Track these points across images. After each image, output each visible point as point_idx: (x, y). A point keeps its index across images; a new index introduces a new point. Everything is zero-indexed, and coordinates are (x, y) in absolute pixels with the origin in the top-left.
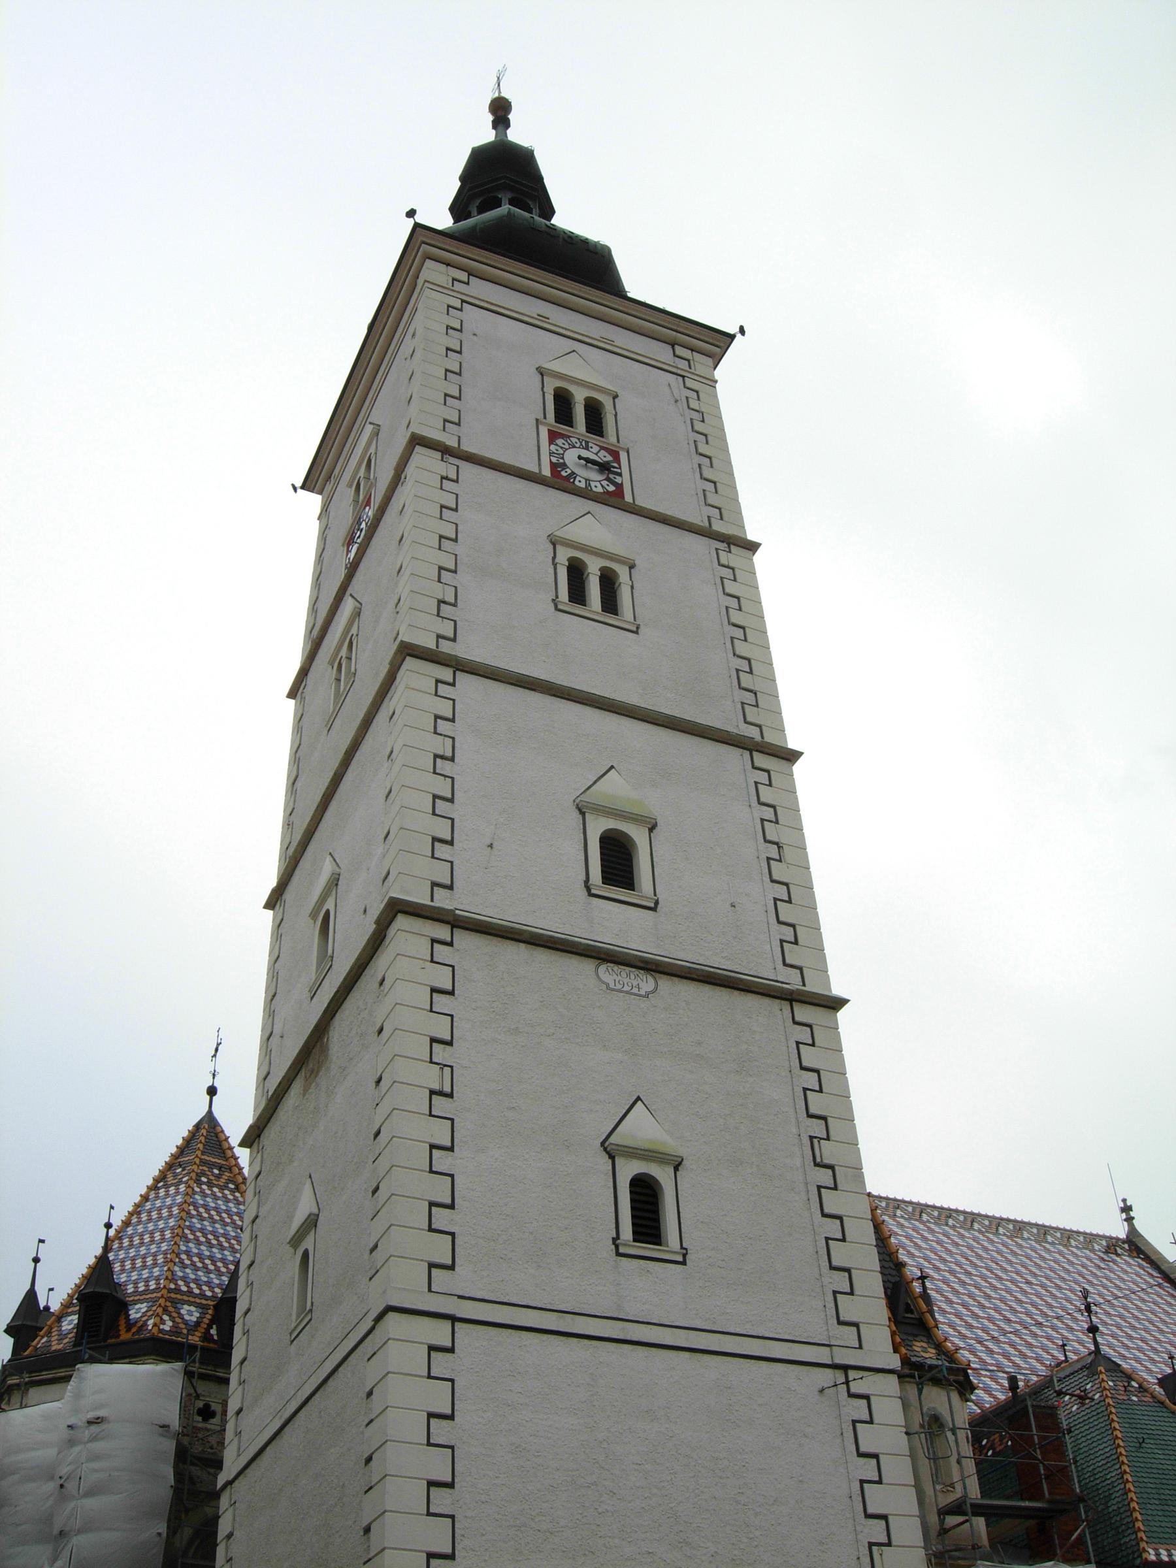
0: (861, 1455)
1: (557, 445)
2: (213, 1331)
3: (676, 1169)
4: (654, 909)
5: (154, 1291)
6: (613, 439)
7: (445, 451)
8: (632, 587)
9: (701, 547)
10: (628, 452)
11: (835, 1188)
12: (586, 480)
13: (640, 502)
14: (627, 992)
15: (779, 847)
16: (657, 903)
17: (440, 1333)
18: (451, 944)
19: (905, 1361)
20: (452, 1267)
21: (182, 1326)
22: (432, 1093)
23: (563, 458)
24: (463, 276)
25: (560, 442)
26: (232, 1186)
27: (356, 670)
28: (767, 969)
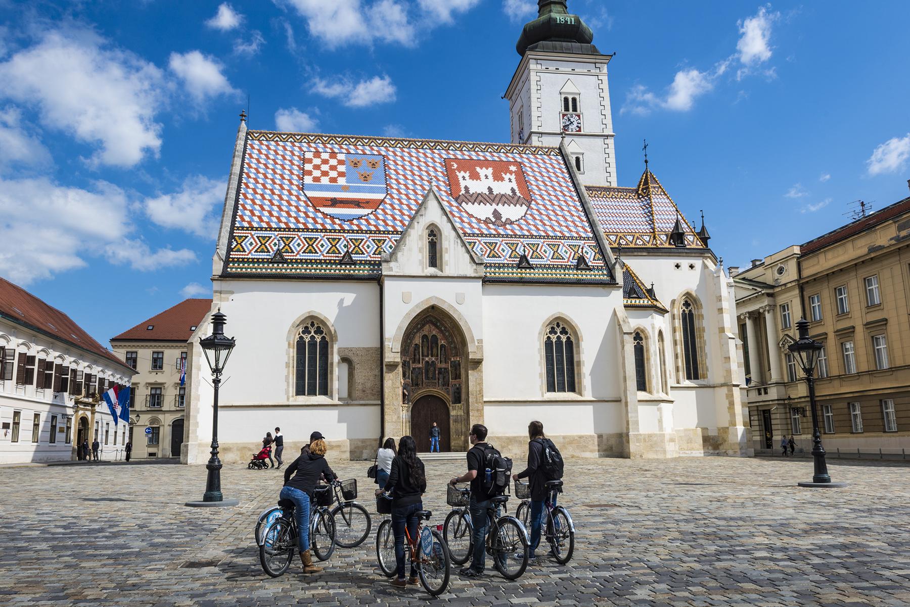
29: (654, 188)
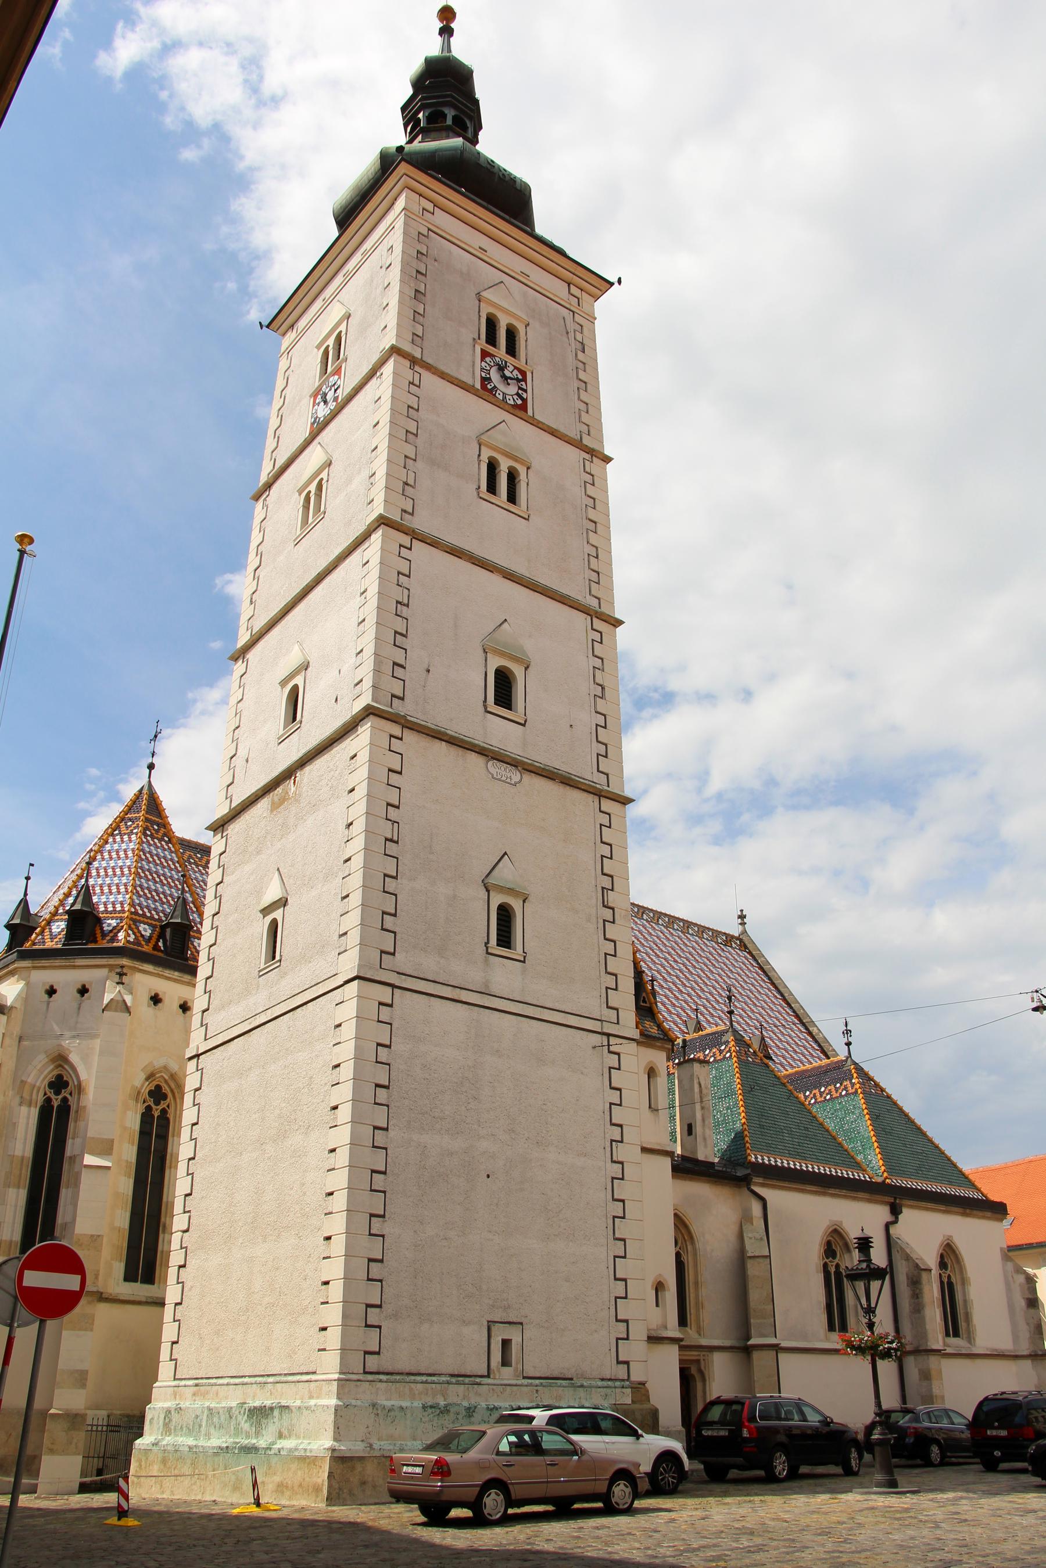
0: (612, 1088)
1: (486, 362)
2: (161, 944)
3: (524, 901)
4: (524, 725)
5: (119, 912)
6: (523, 360)
8: (528, 484)
9: (574, 455)
10: (532, 373)
11: (613, 922)
12: (503, 393)
14: (503, 781)
15: (602, 688)
16: (526, 721)
18: (401, 739)
19: (642, 1034)
20: (393, 954)
21: (141, 939)
22: (387, 839)
23: (489, 374)
24: (430, 206)
25: (488, 359)
26: (166, 839)
28: (583, 769)
29: (153, 823)
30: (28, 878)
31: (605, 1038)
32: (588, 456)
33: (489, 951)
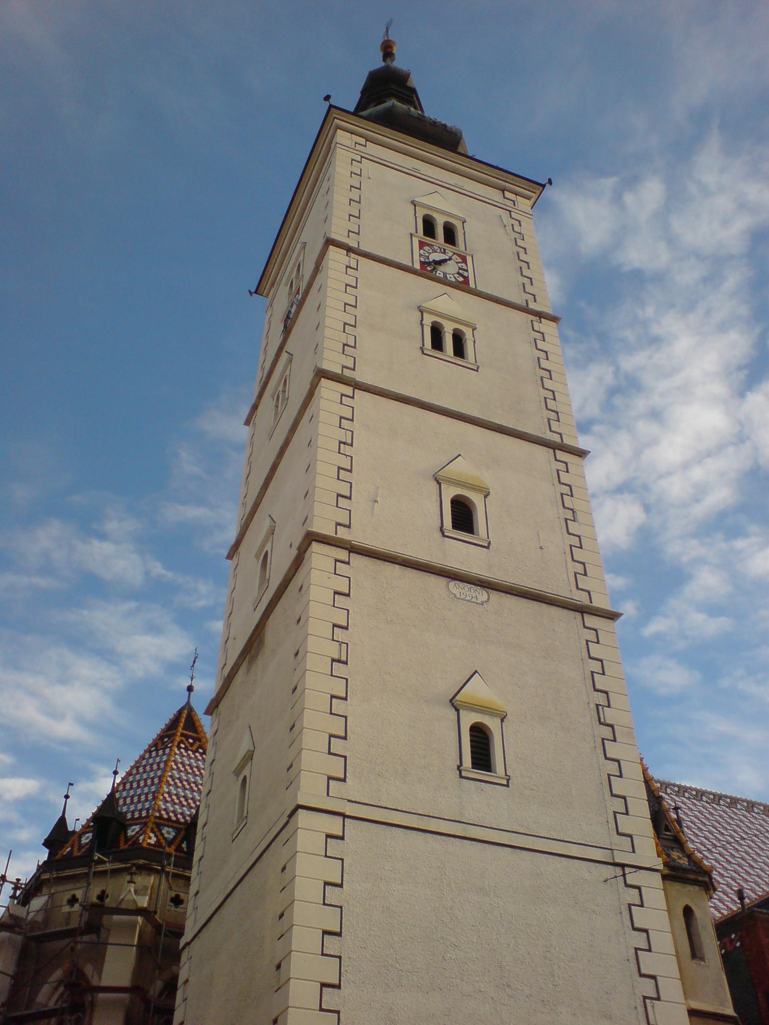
0: (635, 929)
2: (184, 845)
3: (502, 721)
4: (487, 547)
6: (462, 248)
7: (349, 250)
8: (474, 342)
10: (472, 257)
13: (480, 288)
14: (468, 601)
15: (573, 512)
16: (489, 543)
17: (334, 825)
18: (348, 563)
19: (666, 864)
20: (344, 780)
22: (333, 660)
24: (362, 141)
25: (426, 248)
26: (201, 751)
27: (288, 397)
30: (67, 797)
31: (619, 871)
32: (533, 318)
33: (464, 774)
